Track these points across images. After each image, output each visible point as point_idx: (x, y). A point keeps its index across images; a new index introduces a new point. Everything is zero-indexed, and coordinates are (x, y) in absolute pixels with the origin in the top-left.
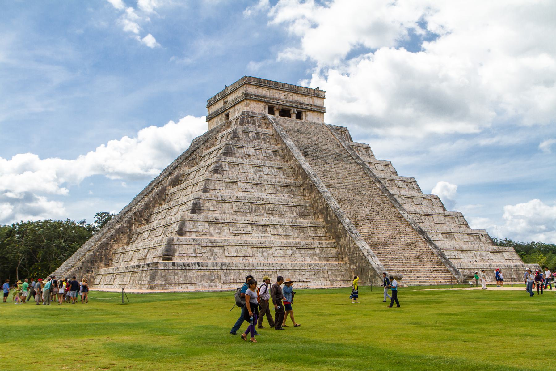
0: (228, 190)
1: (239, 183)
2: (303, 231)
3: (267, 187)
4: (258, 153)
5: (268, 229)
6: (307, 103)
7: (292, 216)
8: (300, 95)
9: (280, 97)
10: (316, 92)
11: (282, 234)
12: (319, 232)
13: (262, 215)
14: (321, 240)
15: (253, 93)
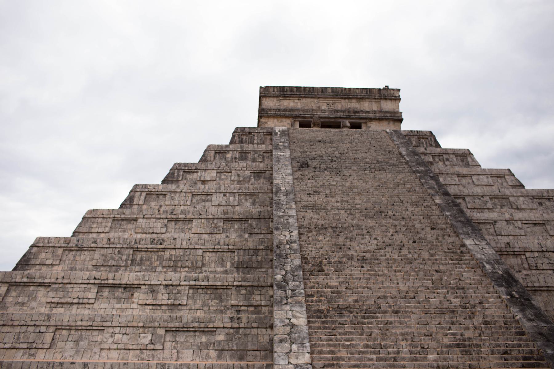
0: (115, 232)
1: (140, 220)
2: (220, 298)
3: (195, 223)
4: (223, 177)
5: (136, 295)
6: (368, 109)
7: (219, 269)
8: (354, 101)
9: (319, 107)
10: (385, 93)
11: (165, 302)
12: (258, 298)
13: (154, 269)
14: (259, 313)
15: (273, 108)
